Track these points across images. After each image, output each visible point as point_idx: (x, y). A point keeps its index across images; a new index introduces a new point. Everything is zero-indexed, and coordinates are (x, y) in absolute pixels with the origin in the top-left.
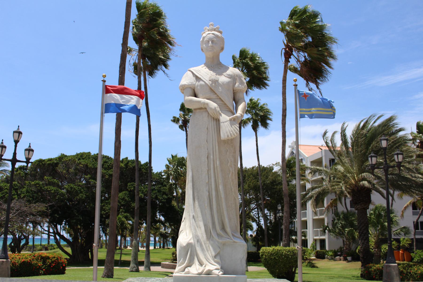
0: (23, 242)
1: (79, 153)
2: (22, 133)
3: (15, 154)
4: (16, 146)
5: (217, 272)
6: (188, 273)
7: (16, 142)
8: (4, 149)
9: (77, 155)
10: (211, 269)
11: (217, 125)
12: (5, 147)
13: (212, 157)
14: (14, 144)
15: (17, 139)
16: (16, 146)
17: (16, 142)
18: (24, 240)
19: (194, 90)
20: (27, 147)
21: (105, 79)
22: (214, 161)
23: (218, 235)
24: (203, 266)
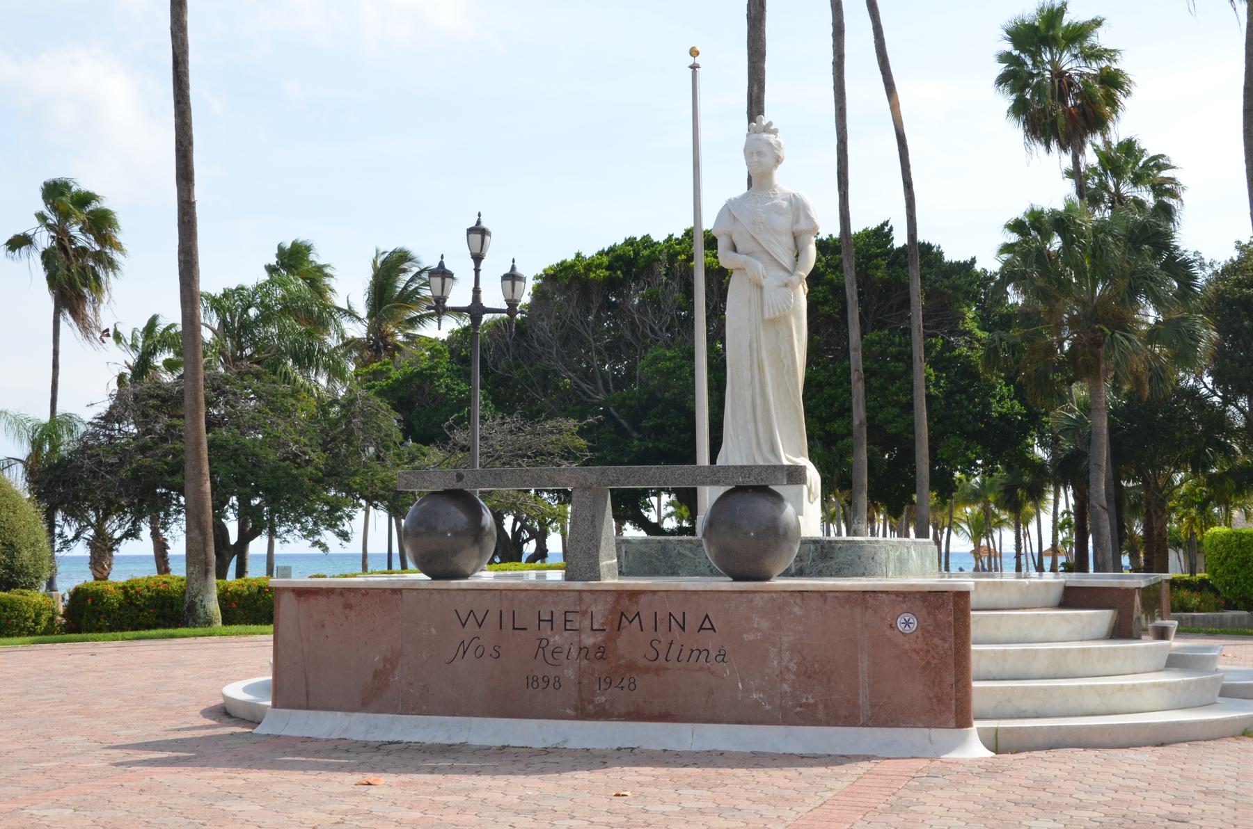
2: (489, 234)
3: (477, 291)
4: (477, 271)
7: (477, 259)
8: (447, 280)
12: (451, 275)
14: (472, 263)
15: (478, 251)
16: (477, 271)
17: (477, 259)
19: (731, 237)
20: (508, 270)
21: (698, 60)
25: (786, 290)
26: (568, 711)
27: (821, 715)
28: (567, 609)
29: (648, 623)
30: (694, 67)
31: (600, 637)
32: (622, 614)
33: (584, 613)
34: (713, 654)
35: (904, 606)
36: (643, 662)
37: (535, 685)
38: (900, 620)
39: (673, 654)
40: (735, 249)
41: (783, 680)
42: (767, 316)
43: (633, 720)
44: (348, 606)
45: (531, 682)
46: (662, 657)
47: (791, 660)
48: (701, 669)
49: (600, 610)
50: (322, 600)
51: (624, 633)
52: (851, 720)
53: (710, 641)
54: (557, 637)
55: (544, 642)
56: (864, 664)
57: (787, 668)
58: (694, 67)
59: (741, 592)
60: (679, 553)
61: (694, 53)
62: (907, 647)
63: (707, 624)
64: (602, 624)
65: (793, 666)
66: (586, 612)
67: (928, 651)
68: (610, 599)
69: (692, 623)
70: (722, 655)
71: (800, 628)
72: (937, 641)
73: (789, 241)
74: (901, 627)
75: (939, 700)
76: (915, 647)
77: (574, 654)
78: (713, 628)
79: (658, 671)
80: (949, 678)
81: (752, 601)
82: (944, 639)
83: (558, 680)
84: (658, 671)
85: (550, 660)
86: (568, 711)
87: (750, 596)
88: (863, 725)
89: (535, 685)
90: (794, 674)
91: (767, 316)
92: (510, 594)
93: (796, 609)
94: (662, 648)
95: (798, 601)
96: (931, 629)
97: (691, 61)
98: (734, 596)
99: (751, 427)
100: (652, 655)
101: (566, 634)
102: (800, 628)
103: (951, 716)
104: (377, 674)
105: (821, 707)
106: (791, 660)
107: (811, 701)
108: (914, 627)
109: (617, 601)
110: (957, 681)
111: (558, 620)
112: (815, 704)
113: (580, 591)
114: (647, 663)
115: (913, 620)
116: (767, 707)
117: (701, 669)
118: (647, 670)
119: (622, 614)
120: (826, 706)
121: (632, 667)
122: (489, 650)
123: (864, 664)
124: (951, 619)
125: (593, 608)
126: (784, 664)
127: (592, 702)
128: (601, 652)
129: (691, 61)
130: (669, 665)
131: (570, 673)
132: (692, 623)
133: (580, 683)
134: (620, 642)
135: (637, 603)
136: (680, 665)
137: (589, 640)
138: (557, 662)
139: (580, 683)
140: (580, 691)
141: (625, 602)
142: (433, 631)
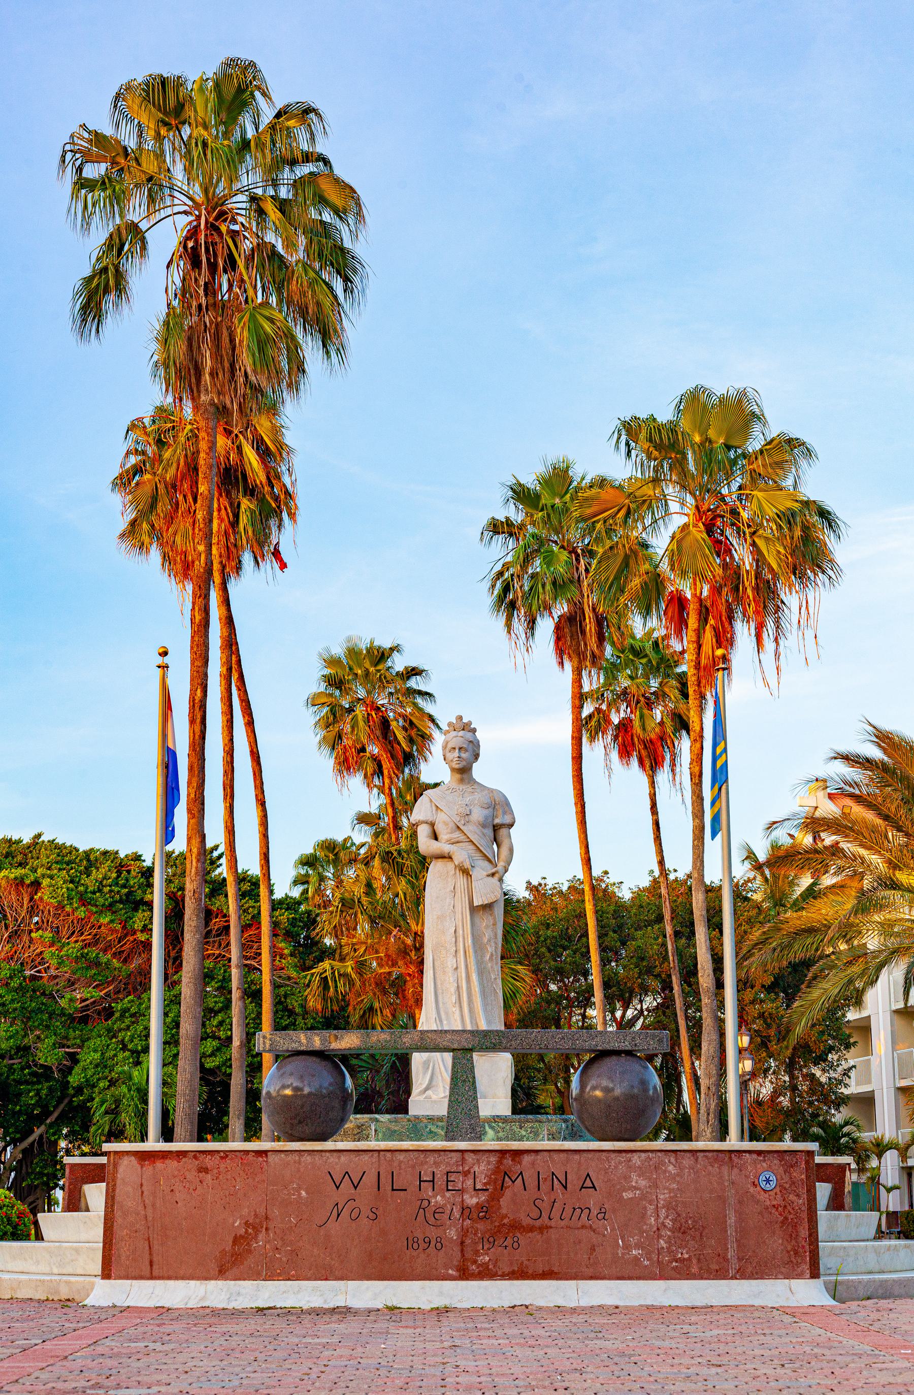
25: (490, 878)
26: (450, 1272)
27: (695, 1270)
28: (448, 1169)
29: (531, 1182)
30: (164, 667)
31: (483, 1197)
32: (505, 1173)
33: (466, 1174)
34: (595, 1212)
35: (764, 1164)
36: (526, 1221)
37: (416, 1246)
38: (762, 1178)
39: (556, 1214)
40: (436, 838)
41: (659, 1237)
43: (517, 1279)
44: (205, 1170)
45: (411, 1243)
46: (545, 1215)
47: (667, 1217)
48: (583, 1227)
49: (482, 1169)
50: (172, 1164)
51: (508, 1193)
52: (721, 1274)
53: (592, 1200)
54: (439, 1198)
55: (425, 1203)
56: (732, 1220)
57: (663, 1223)
58: (164, 667)
59: (620, 1151)
60: (431, 1132)
62: (768, 1203)
63: (588, 1183)
64: (485, 1184)
65: (669, 1223)
66: (469, 1171)
67: (785, 1207)
68: (493, 1159)
69: (574, 1181)
70: (603, 1212)
71: (675, 1186)
72: (792, 1197)
73: (489, 832)
74: (763, 1184)
75: (796, 1253)
76: (775, 1203)
77: (457, 1214)
78: (594, 1187)
79: (542, 1229)
80: (804, 1233)
81: (630, 1160)
82: (798, 1196)
83: (439, 1240)
84: (542, 1229)
85: (432, 1220)
86: (450, 1272)
87: (629, 1155)
88: (732, 1278)
89: (416, 1246)
90: (670, 1230)
92: (389, 1155)
93: (671, 1168)
94: (545, 1206)
95: (673, 1160)
96: (787, 1186)
97: (160, 660)
98: (613, 1155)
100: (536, 1213)
101: (448, 1194)
102: (675, 1186)
103: (806, 1267)
104: (236, 1240)
105: (694, 1261)
106: (667, 1217)
107: (686, 1256)
108: (773, 1184)
109: (500, 1162)
110: (810, 1235)
111: (440, 1181)
112: (689, 1259)
113: (462, 1151)
114: (531, 1222)
115: (773, 1178)
116: (646, 1263)
117: (583, 1227)
118: (531, 1229)
119: (505, 1173)
120: (699, 1260)
121: (516, 1226)
122: (366, 1212)
123: (732, 1220)
124: (803, 1176)
125: (476, 1169)
126: (660, 1221)
127: (475, 1262)
128: (485, 1211)
129: (160, 660)
130: (553, 1223)
131: (453, 1234)
132: (574, 1181)
133: (462, 1243)
134: (503, 1202)
135: (520, 1163)
136: (562, 1223)
137: (472, 1200)
138: (439, 1223)
139: (462, 1243)
140: (462, 1251)
141: (508, 1161)
142: (303, 1193)
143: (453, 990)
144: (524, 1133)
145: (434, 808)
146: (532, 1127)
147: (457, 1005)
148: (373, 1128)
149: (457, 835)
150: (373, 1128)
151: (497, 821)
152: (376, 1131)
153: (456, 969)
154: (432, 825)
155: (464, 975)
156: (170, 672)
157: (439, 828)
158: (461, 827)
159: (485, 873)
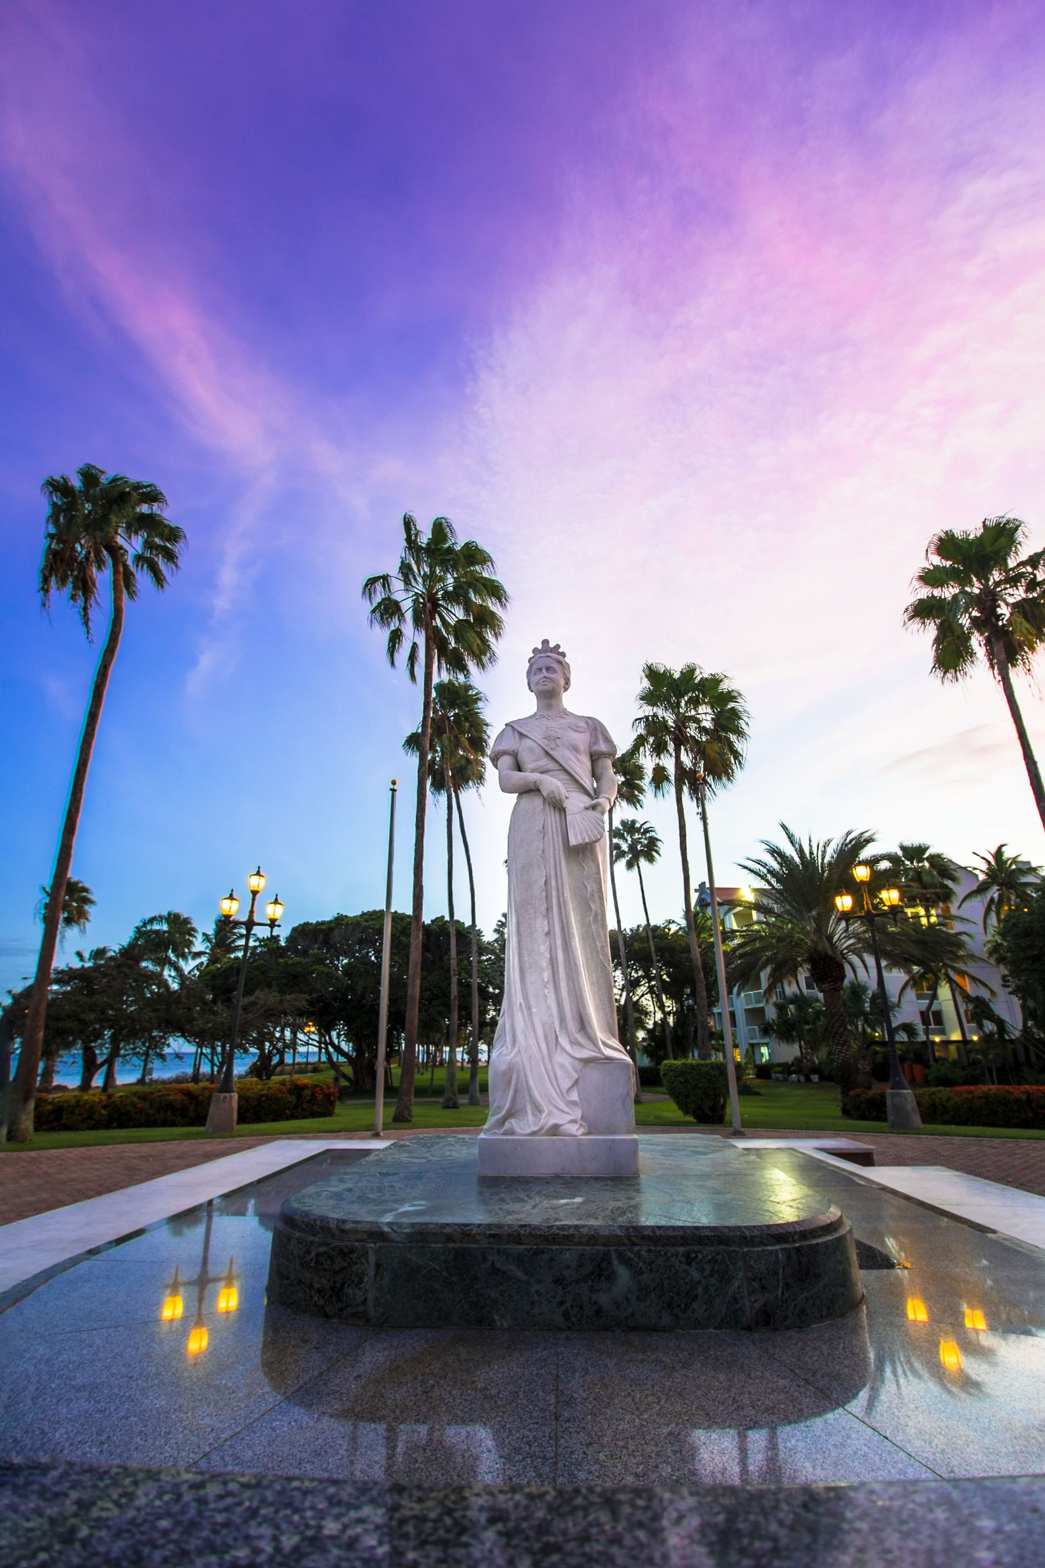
0: (276, 1059)
1: (365, 911)
3: (252, 912)
4: (254, 900)
5: (573, 1129)
6: (512, 1132)
9: (364, 914)
10: (561, 1122)
11: (561, 821)
13: (553, 883)
16: (254, 900)
18: (278, 1056)
21: (396, 787)
22: (558, 890)
23: (574, 1043)
24: (544, 1115)
25: (590, 813)
30: (393, 790)
42: (573, 842)
58: (393, 790)
60: (495, 1271)
61: (394, 783)
91: (573, 842)
97: (392, 786)
99: (551, 996)
143: (544, 963)
144: (696, 1275)
145: (517, 735)
146: (713, 1261)
147: (551, 986)
148: (372, 1258)
149: (545, 762)
150: (372, 1258)
151: (595, 748)
152: (378, 1266)
153: (548, 934)
154: (515, 755)
155: (559, 942)
156: (397, 793)
157: (525, 758)
158: (551, 752)
159: (582, 806)
